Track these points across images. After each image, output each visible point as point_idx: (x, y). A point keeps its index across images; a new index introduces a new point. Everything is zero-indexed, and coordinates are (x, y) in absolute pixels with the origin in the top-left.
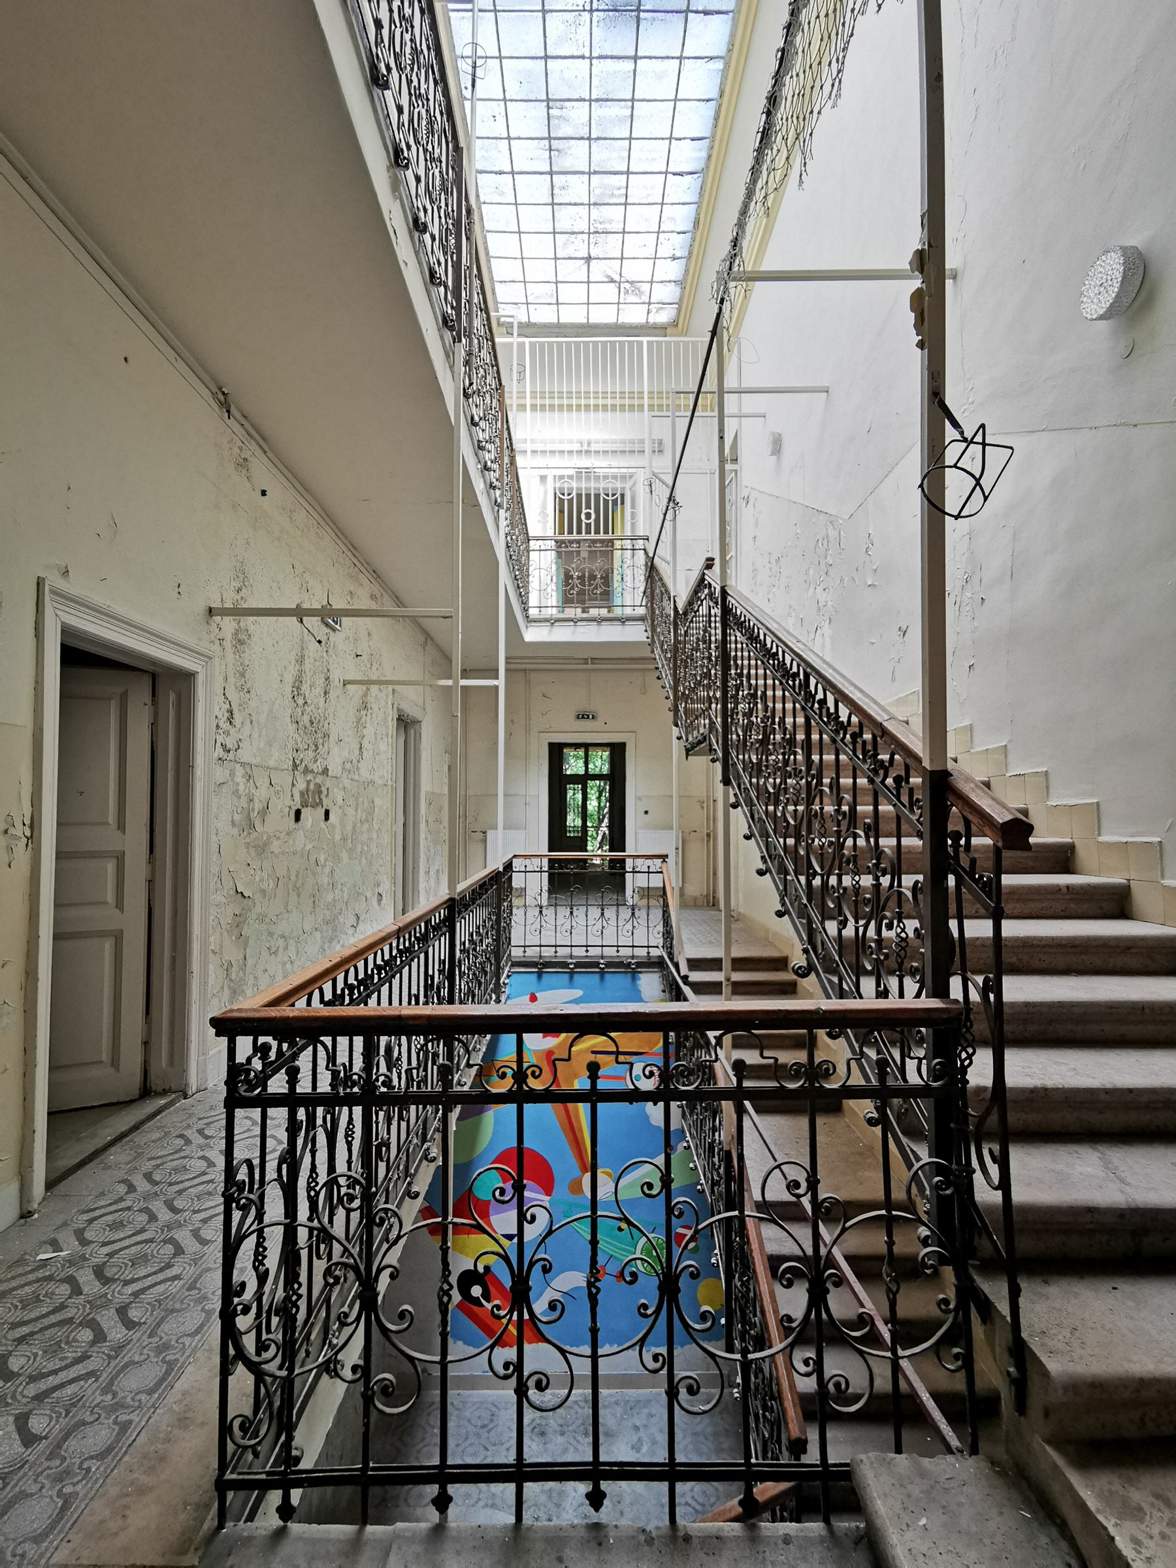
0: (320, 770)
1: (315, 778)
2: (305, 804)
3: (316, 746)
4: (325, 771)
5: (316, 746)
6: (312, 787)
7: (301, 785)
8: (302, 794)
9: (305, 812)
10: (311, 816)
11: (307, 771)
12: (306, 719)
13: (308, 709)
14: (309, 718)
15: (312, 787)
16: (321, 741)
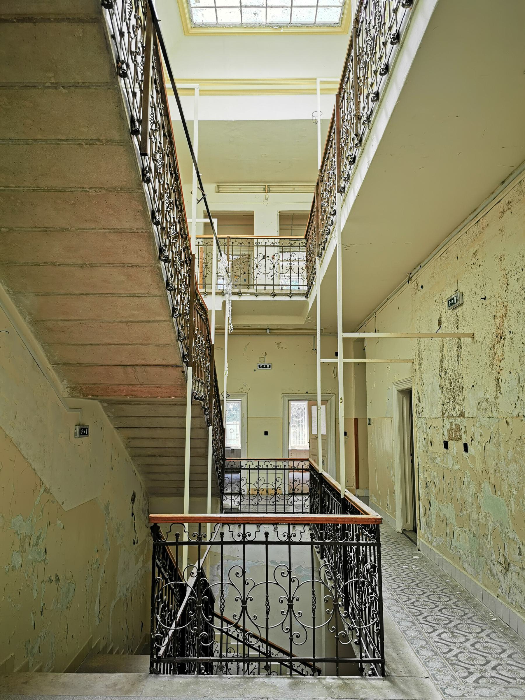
0: (458, 414)
1: (455, 421)
2: (451, 439)
3: (454, 398)
4: (462, 414)
5: (454, 398)
6: (454, 426)
7: (448, 426)
8: (449, 431)
9: (450, 443)
10: (455, 447)
11: (450, 417)
12: (447, 382)
13: (447, 375)
14: (449, 381)
15: (454, 426)
16: (457, 393)
